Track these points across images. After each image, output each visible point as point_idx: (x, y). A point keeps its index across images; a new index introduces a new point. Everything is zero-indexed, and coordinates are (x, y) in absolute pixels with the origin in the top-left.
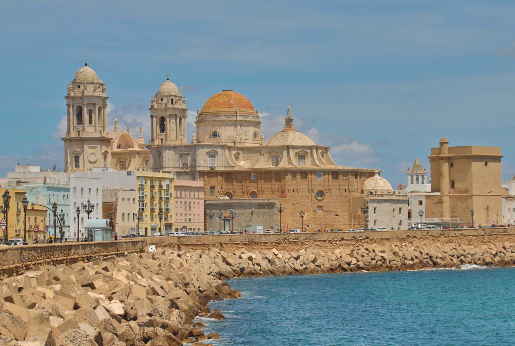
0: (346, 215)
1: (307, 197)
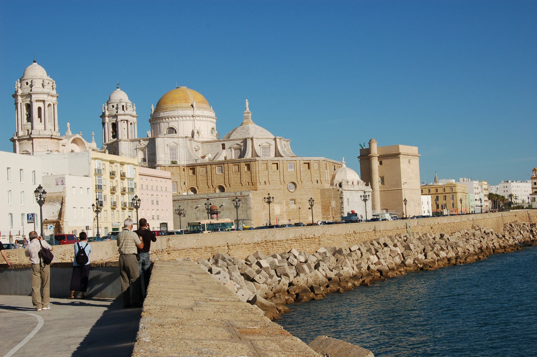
0: (319, 208)
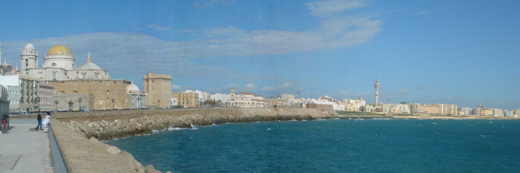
1: (102, 93)
